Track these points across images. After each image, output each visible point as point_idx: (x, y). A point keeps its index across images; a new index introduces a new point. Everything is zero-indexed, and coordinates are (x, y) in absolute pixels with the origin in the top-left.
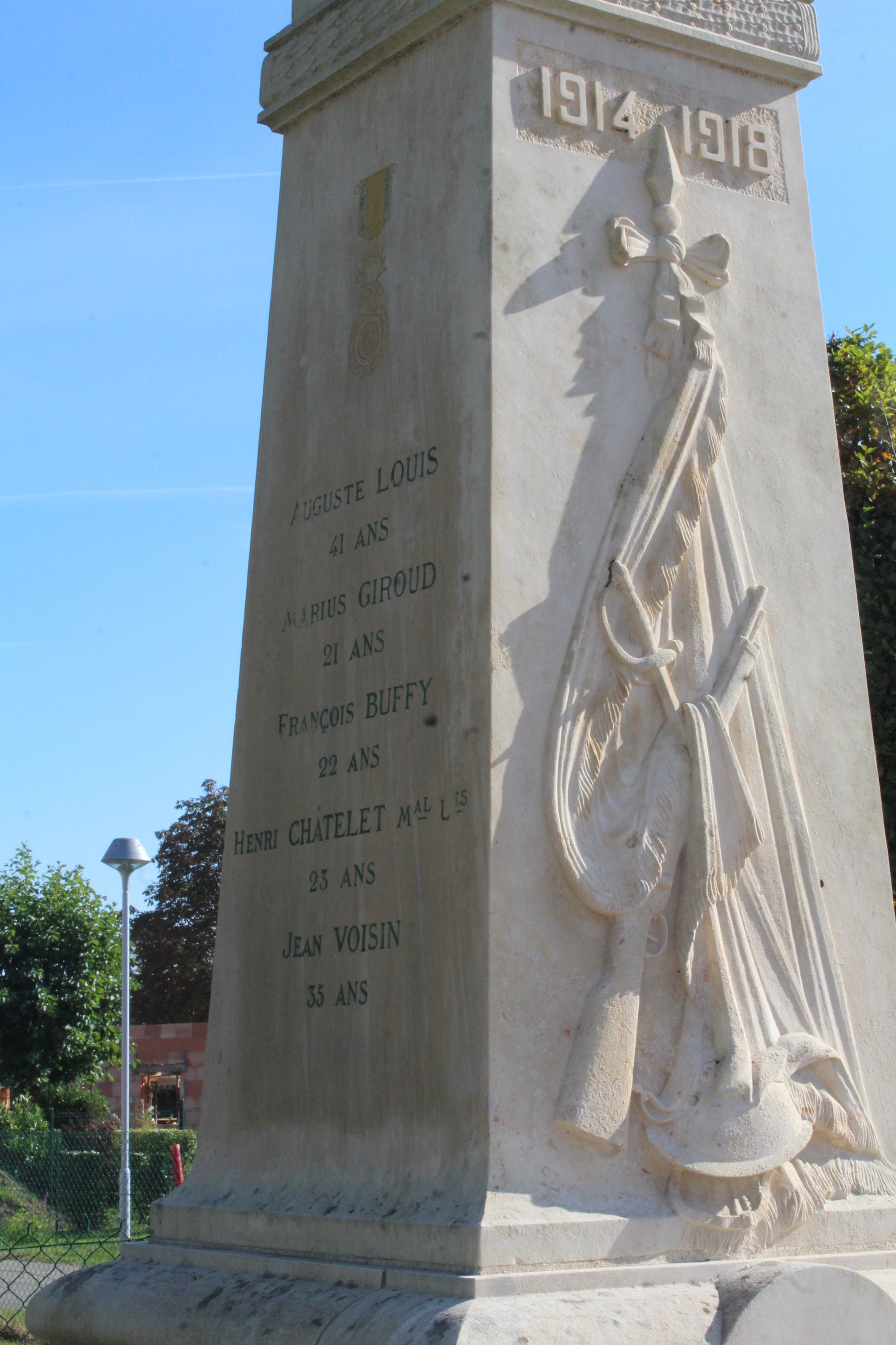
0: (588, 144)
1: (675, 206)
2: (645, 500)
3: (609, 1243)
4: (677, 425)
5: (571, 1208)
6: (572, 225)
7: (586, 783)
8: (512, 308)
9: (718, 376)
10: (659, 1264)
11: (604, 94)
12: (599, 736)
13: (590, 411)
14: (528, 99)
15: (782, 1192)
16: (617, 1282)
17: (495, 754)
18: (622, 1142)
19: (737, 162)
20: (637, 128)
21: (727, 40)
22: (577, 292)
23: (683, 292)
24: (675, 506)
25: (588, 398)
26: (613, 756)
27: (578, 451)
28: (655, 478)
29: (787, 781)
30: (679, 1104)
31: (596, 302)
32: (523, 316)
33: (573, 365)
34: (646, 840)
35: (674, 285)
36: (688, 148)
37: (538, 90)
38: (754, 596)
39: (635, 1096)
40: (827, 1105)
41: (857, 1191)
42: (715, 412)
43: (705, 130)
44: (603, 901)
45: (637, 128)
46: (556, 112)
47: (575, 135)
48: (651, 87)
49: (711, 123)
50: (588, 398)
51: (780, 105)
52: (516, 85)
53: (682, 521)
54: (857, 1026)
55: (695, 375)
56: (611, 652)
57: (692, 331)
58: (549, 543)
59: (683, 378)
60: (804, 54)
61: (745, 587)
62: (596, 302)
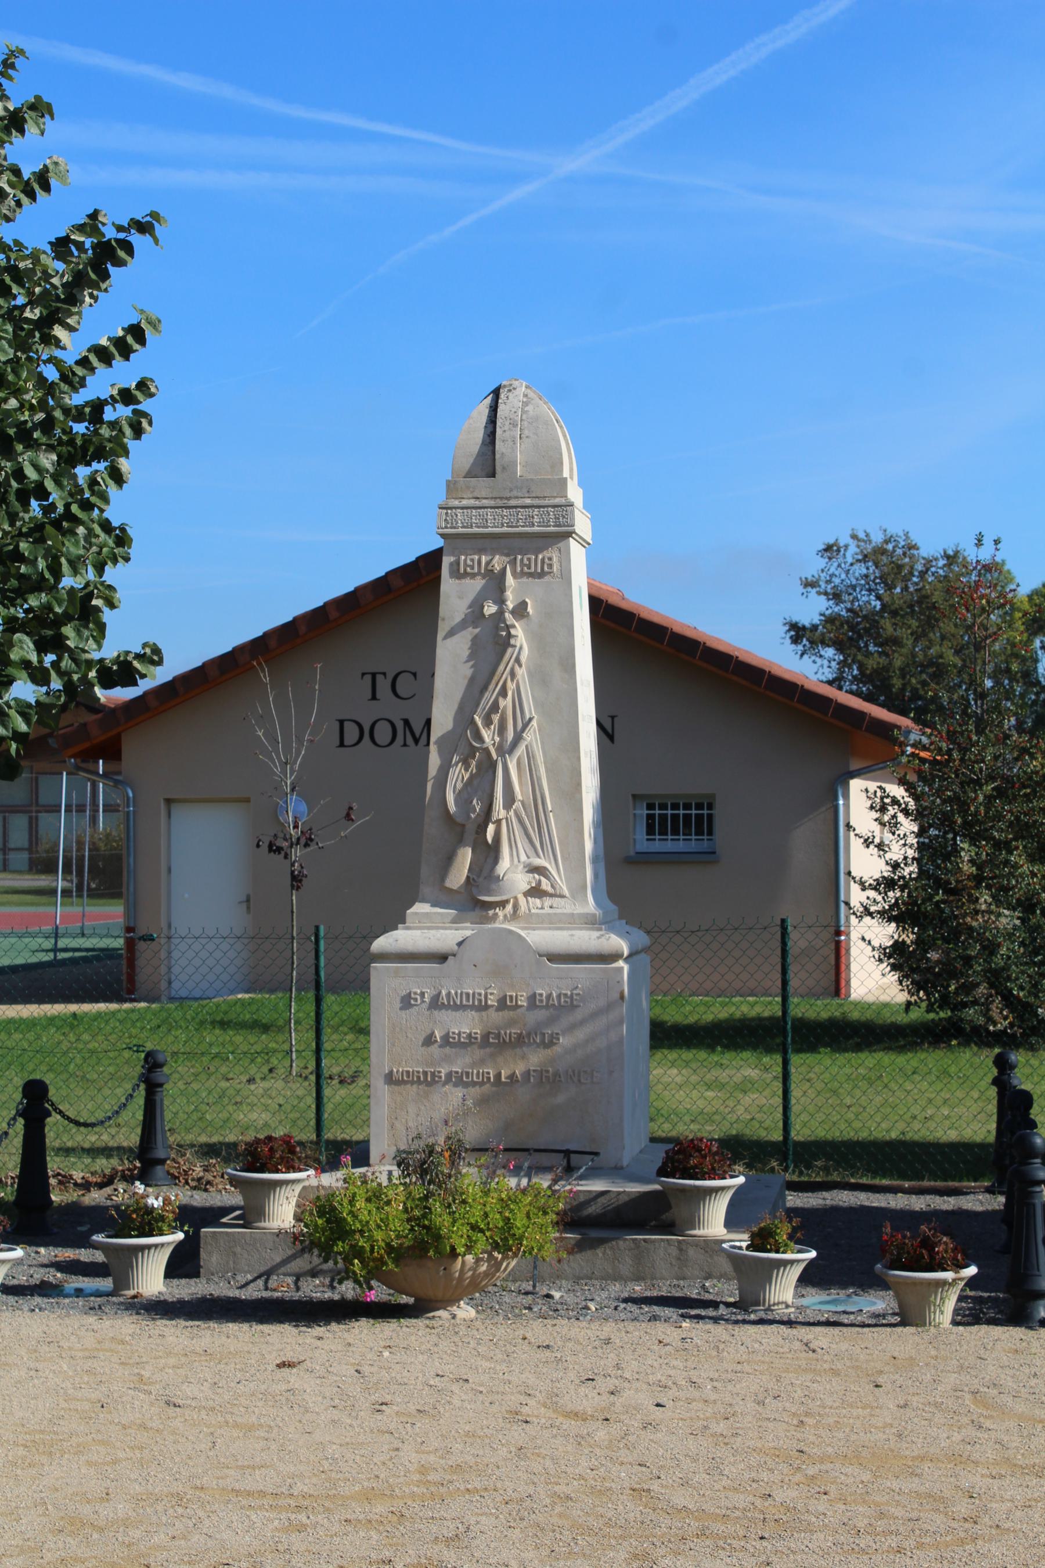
0: (479, 577)
1: (509, 594)
2: (487, 695)
3: (450, 918)
4: (501, 667)
5: (441, 908)
6: (470, 607)
7: (459, 786)
8: (445, 638)
9: (521, 648)
10: (468, 925)
11: (484, 559)
12: (466, 770)
13: (472, 667)
14: (455, 567)
15: (516, 907)
16: (450, 928)
17: (429, 777)
18: (463, 890)
19: (539, 570)
20: (498, 568)
21: (536, 529)
22: (470, 629)
23: (508, 623)
24: (499, 694)
25: (471, 663)
26: (472, 776)
27: (466, 682)
28: (491, 687)
29: (539, 779)
30: (481, 879)
31: (477, 630)
32: (448, 640)
33: (467, 653)
34: (475, 802)
35: (504, 621)
36: (519, 569)
37: (458, 564)
38: (531, 719)
39: (468, 877)
40: (540, 881)
41: (551, 907)
42: (518, 661)
43: (526, 561)
44: (459, 820)
45: (498, 568)
46: (465, 570)
47: (473, 576)
48: (506, 551)
49: (529, 559)
50: (471, 663)
51: (561, 545)
52: (451, 564)
53: (501, 700)
54: (562, 856)
55: (510, 650)
56: (471, 744)
57: (509, 635)
58: (453, 713)
59: (504, 652)
60: (568, 526)
61: (528, 717)
62: (477, 630)
